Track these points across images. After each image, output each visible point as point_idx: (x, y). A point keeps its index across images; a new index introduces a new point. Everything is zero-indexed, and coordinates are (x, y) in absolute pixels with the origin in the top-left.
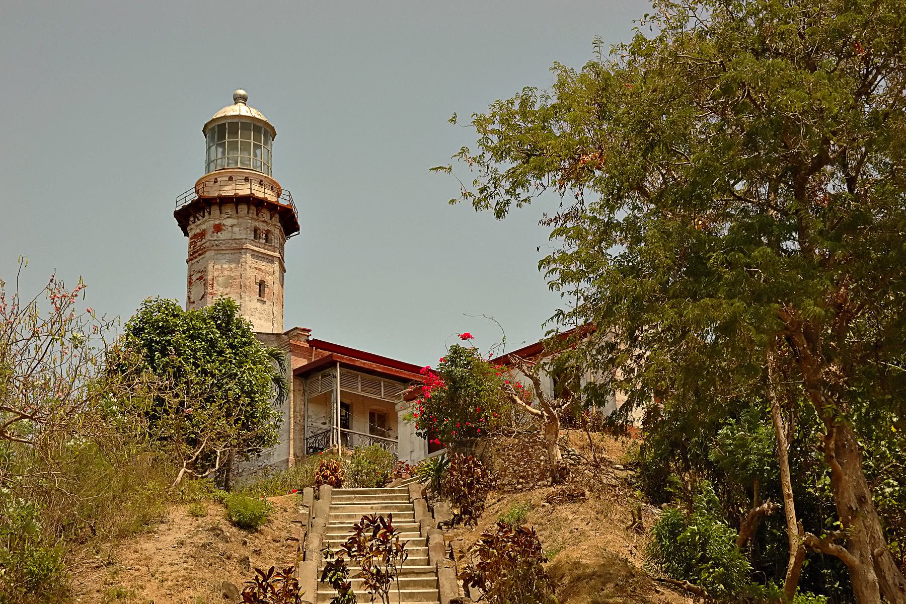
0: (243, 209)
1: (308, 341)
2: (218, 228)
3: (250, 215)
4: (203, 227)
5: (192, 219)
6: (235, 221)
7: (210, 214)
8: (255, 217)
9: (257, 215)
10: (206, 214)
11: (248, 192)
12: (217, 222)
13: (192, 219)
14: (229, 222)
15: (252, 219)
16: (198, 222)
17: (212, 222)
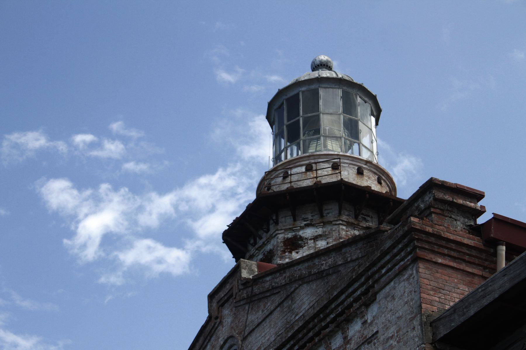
0: (331, 211)
1: (476, 230)
2: (294, 244)
3: (344, 218)
4: (269, 247)
5: (252, 241)
6: (319, 231)
7: (277, 223)
8: (352, 220)
9: (356, 218)
10: (272, 227)
11: (334, 179)
12: (290, 235)
13: (252, 241)
14: (309, 232)
15: (349, 224)
16: (260, 243)
17: (281, 236)
